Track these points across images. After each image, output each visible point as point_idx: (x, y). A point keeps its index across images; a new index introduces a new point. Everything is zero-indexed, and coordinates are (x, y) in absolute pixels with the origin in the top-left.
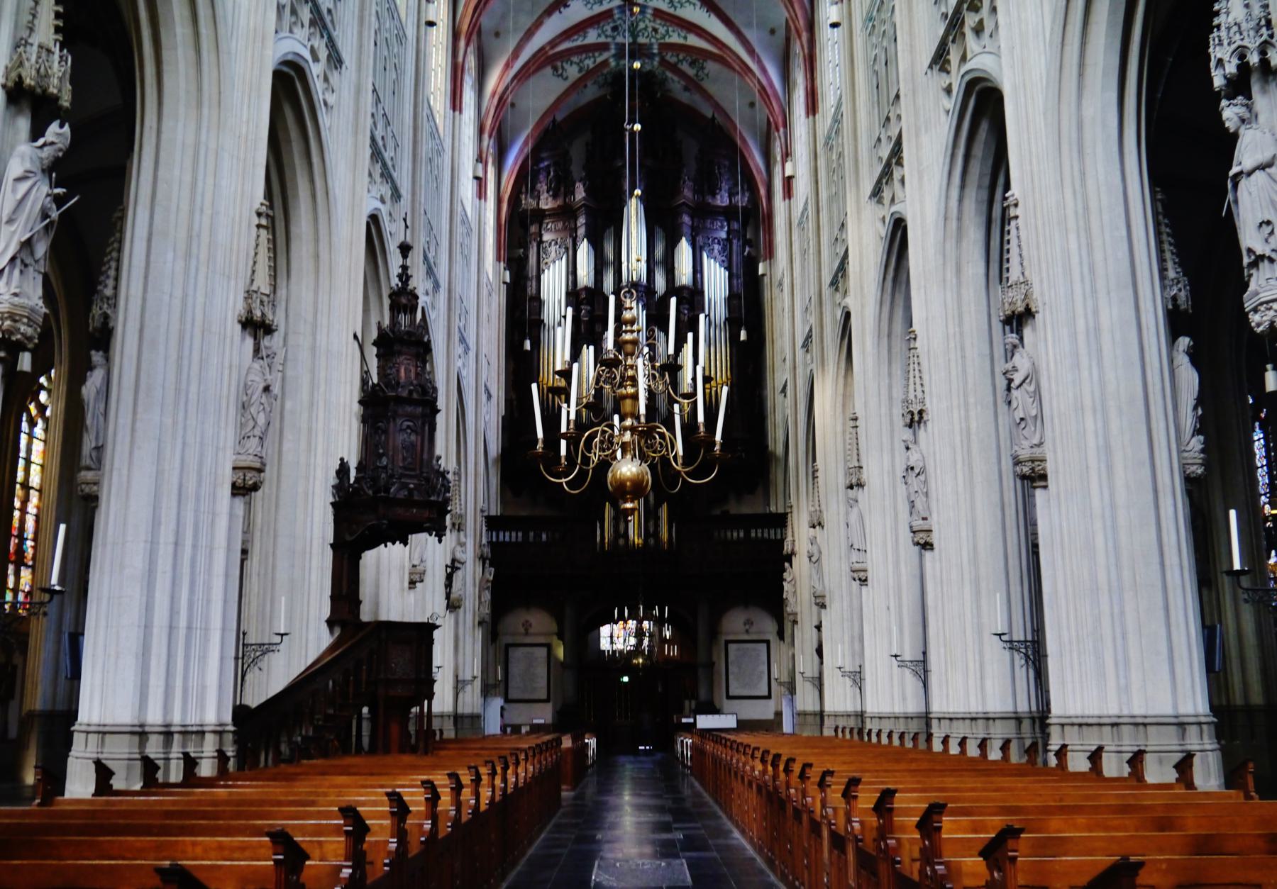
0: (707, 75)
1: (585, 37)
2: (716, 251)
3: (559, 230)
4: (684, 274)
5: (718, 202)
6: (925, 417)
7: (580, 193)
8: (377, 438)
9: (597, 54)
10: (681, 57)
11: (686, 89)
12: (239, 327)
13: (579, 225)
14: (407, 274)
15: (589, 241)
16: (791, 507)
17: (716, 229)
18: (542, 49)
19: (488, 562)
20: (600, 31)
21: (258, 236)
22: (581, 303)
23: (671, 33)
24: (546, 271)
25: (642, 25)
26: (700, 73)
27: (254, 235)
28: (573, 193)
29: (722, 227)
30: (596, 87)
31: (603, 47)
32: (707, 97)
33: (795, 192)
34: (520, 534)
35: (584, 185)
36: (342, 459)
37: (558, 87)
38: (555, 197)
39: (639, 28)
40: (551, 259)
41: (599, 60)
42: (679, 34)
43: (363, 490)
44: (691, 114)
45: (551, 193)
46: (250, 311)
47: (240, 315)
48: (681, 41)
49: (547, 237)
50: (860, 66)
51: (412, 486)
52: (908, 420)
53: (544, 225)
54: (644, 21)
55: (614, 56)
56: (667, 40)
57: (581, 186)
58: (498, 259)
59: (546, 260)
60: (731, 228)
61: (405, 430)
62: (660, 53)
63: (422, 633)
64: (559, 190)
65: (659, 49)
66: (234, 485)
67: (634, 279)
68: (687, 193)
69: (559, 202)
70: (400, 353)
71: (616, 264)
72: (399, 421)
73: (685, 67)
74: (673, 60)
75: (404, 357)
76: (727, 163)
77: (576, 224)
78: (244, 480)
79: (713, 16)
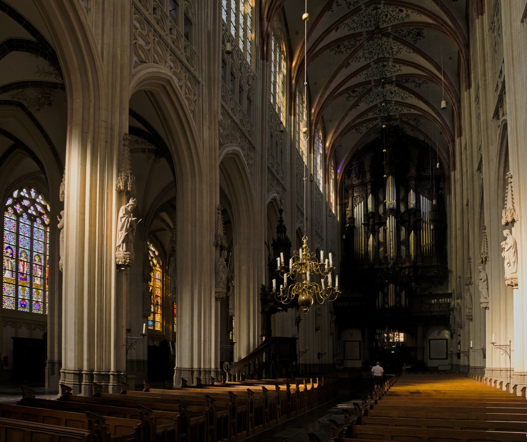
5: (427, 174)
10: (409, 118)
25: (391, 108)
26: (418, 123)
31: (376, 119)
41: (374, 124)
48: (408, 112)
55: (381, 121)
56: (402, 112)
68: (413, 172)
73: (411, 122)
74: (406, 119)
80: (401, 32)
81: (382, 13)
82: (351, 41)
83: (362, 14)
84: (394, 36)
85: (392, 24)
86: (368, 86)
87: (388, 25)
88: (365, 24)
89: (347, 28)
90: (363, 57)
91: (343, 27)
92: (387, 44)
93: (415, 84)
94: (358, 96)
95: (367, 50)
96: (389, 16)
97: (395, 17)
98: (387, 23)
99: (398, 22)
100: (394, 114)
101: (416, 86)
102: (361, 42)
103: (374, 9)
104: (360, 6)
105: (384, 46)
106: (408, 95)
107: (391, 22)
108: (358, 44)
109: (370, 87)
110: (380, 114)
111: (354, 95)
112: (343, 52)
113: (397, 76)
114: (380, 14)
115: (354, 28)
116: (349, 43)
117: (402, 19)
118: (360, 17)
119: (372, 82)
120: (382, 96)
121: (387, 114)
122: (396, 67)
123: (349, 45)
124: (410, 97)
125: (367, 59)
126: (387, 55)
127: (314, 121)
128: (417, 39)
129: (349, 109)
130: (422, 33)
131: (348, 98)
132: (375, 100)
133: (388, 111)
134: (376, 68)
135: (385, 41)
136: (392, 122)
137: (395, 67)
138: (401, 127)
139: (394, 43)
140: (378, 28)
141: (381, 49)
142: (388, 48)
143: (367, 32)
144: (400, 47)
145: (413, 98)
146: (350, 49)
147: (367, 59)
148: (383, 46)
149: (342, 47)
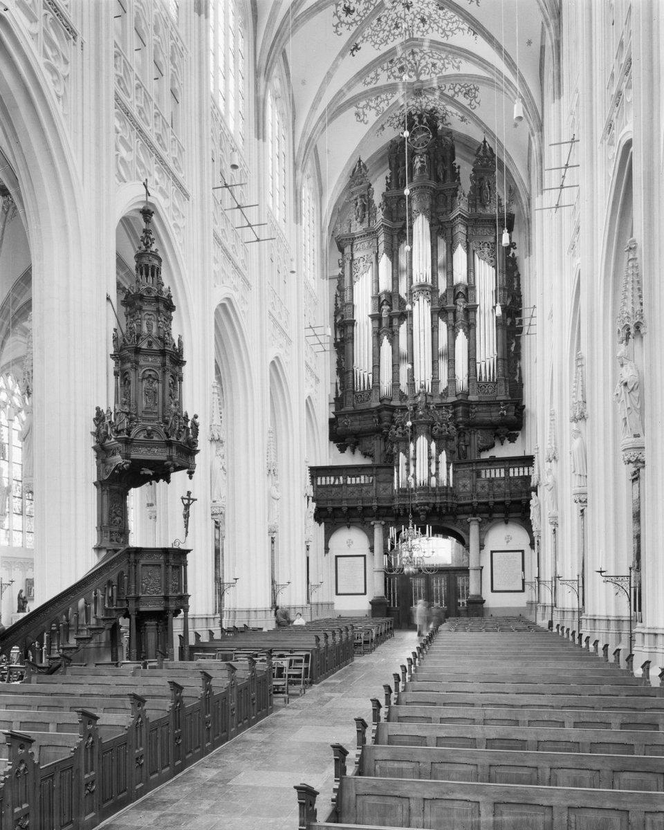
4: (460, 275)
6: (642, 330)
10: (457, 90)
11: (463, 119)
20: (389, 73)
23: (447, 66)
25: (423, 63)
26: (473, 101)
28: (375, 217)
31: (392, 88)
35: (382, 209)
37: (361, 130)
39: (422, 65)
41: (391, 102)
42: (453, 65)
44: (467, 142)
45: (359, 220)
48: (455, 71)
52: (623, 335)
54: (424, 58)
55: (403, 96)
56: (445, 73)
62: (439, 88)
63: (175, 558)
64: (365, 217)
65: (438, 83)
69: (365, 225)
73: (461, 99)
74: (450, 93)
77: (378, 243)
79: (479, 37)
94: (356, 22)
100: (428, 77)
111: (349, 19)
121: (414, 79)
127: (264, 63)
131: (337, 26)
132: (392, 38)
133: (417, 68)
138: (441, 112)
145: (466, 32)
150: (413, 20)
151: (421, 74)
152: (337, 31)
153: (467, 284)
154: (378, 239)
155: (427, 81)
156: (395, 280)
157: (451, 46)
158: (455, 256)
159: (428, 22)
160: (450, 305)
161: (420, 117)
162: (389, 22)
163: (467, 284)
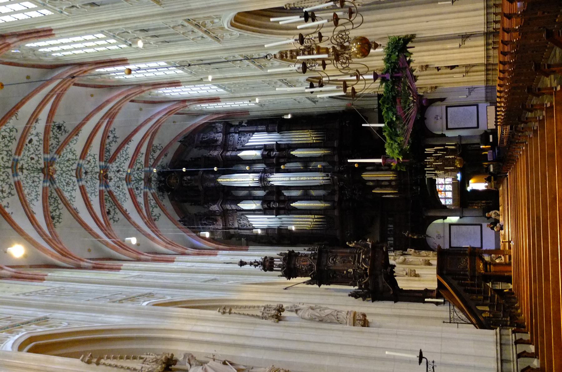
0: (160, 144)
1: (141, 203)
2: (244, 139)
3: (233, 219)
4: (257, 154)
7: (215, 208)
8: (338, 276)
9: (149, 199)
10: (151, 157)
12: (280, 322)
13: (230, 208)
14: (254, 262)
15: (239, 203)
16: (375, 92)
17: (234, 139)
18: (146, 223)
19: (404, 252)
20: (138, 196)
21: (235, 313)
22: (269, 207)
23: (140, 161)
24: (253, 225)
25: (136, 175)
27: (234, 315)
28: (215, 211)
29: (233, 136)
30: (164, 200)
31: (145, 195)
32: (170, 144)
33: (216, 96)
34: (389, 239)
35: (211, 205)
36: (349, 295)
37: (163, 218)
38: (216, 221)
39: (137, 177)
40: (247, 223)
41: (151, 197)
42: (141, 157)
43: (365, 283)
45: (215, 223)
46: (273, 316)
47: (274, 322)
48: (144, 156)
49: (236, 225)
50: (159, 52)
51: (363, 257)
53: (230, 227)
55: (150, 190)
56: (143, 163)
57: (212, 207)
58: (247, 250)
59: (248, 225)
60: (233, 131)
61: (334, 262)
66: (364, 326)
67: (257, 179)
68: (215, 153)
70: (295, 264)
71: (249, 189)
72: (330, 264)
73: (156, 155)
74: (152, 161)
75: (296, 263)
76: (202, 134)
77: (230, 210)
78: (360, 320)
79: (133, 138)
80: (53, 146)
81: (28, 163)
82: (50, 203)
83: (24, 184)
84: (56, 153)
85: (42, 153)
86: (106, 195)
87: (42, 158)
88: (35, 183)
89: (35, 202)
90: (71, 193)
91: (31, 206)
92: (63, 165)
93: (113, 142)
95: (64, 187)
96: (33, 156)
97: (35, 149)
98: (40, 159)
99: (42, 146)
100: (143, 173)
101: (116, 141)
102: (53, 191)
103: (22, 172)
104: (15, 183)
105: (64, 169)
106: (124, 152)
107: (40, 154)
108: (55, 195)
109: (107, 193)
110: (141, 189)
111: (112, 213)
112: (60, 213)
113: (100, 160)
114: (29, 166)
115: (37, 195)
116: (52, 205)
117: (39, 141)
118: (27, 187)
119: (101, 188)
120: (120, 182)
121: (143, 182)
122: (90, 159)
123: (53, 205)
124: (126, 150)
125: (74, 189)
126: (75, 167)
128: (64, 129)
129: (128, 220)
130: (59, 124)
131: (114, 221)
132: (124, 190)
133: (138, 179)
134: (87, 182)
135: (59, 166)
136: (153, 179)
137: (89, 162)
139: (63, 157)
140: (42, 170)
141: (66, 173)
142: (67, 164)
143: (44, 182)
144: (69, 150)
145: (129, 146)
146: (59, 204)
147: (74, 189)
148: (63, 169)
149: (54, 214)
150: (117, 177)
151: (141, 177)
152: (117, 221)
153: (262, 150)
154: (228, 210)
155: (145, 174)
156: (254, 198)
157: (133, 155)
158: (244, 158)
159: (120, 168)
160: (274, 161)
161: (160, 182)
162: (116, 191)
163: (262, 150)
